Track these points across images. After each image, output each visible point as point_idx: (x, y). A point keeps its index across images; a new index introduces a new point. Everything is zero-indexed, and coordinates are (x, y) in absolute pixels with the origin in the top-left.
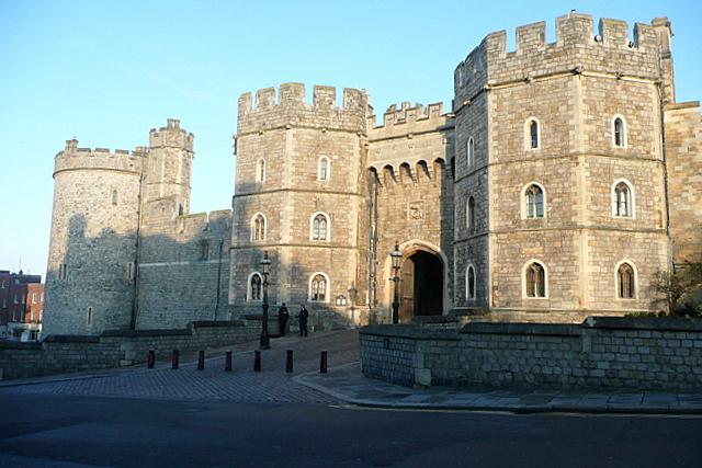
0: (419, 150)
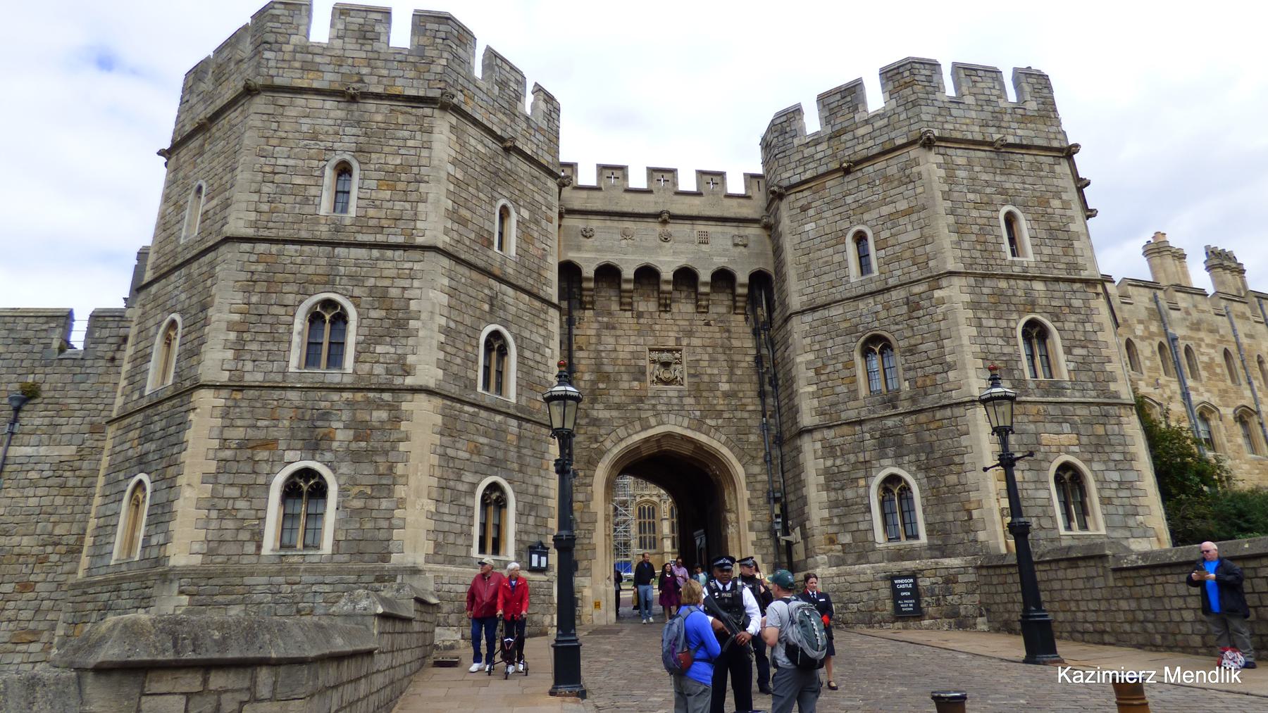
0: (682, 247)
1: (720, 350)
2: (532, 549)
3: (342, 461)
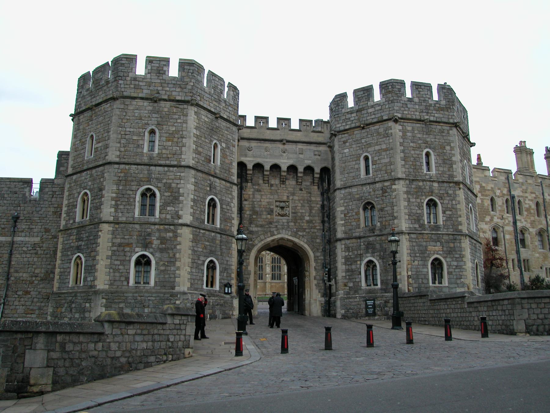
0: (291, 156)
1: (306, 202)
2: (226, 286)
3: (156, 252)
